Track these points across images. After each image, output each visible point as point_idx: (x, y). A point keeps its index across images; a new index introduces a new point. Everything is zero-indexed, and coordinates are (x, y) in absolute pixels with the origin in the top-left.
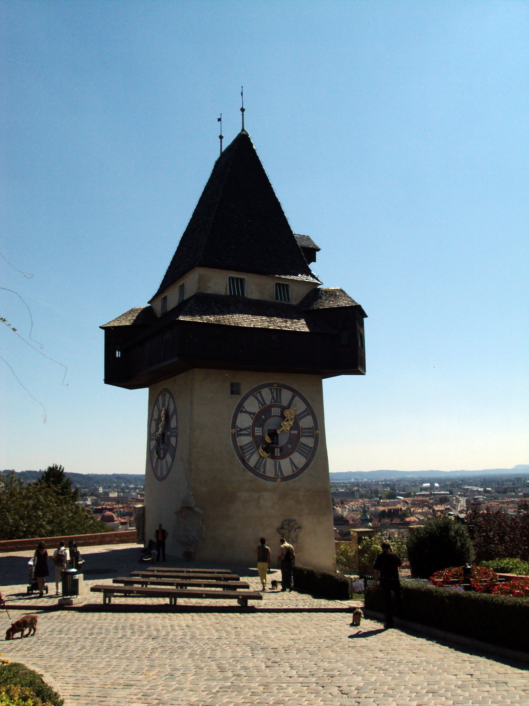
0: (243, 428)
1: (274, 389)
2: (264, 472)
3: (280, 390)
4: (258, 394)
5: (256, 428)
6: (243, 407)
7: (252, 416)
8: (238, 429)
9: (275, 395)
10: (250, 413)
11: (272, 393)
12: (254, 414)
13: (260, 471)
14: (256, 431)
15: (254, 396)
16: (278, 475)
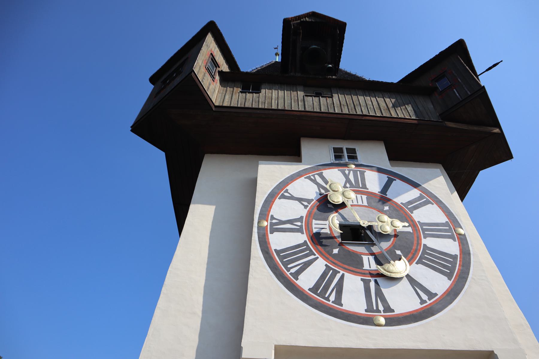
0: (284, 219)
1: (349, 171)
2: (338, 300)
3: (362, 174)
4: (317, 176)
5: (314, 222)
6: (287, 191)
7: (306, 204)
8: (274, 221)
9: (351, 177)
10: (300, 200)
11: (347, 177)
12: (309, 201)
13: (329, 301)
14: (314, 226)
15: (309, 178)
16: (378, 311)
